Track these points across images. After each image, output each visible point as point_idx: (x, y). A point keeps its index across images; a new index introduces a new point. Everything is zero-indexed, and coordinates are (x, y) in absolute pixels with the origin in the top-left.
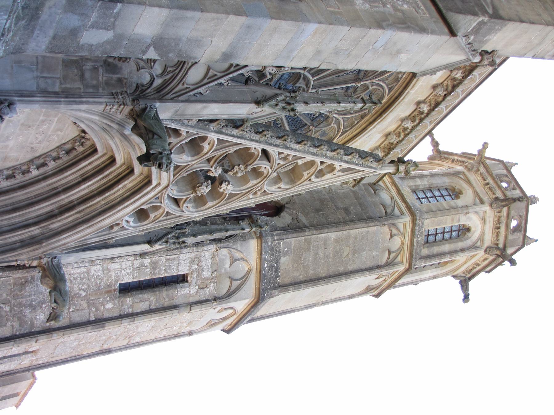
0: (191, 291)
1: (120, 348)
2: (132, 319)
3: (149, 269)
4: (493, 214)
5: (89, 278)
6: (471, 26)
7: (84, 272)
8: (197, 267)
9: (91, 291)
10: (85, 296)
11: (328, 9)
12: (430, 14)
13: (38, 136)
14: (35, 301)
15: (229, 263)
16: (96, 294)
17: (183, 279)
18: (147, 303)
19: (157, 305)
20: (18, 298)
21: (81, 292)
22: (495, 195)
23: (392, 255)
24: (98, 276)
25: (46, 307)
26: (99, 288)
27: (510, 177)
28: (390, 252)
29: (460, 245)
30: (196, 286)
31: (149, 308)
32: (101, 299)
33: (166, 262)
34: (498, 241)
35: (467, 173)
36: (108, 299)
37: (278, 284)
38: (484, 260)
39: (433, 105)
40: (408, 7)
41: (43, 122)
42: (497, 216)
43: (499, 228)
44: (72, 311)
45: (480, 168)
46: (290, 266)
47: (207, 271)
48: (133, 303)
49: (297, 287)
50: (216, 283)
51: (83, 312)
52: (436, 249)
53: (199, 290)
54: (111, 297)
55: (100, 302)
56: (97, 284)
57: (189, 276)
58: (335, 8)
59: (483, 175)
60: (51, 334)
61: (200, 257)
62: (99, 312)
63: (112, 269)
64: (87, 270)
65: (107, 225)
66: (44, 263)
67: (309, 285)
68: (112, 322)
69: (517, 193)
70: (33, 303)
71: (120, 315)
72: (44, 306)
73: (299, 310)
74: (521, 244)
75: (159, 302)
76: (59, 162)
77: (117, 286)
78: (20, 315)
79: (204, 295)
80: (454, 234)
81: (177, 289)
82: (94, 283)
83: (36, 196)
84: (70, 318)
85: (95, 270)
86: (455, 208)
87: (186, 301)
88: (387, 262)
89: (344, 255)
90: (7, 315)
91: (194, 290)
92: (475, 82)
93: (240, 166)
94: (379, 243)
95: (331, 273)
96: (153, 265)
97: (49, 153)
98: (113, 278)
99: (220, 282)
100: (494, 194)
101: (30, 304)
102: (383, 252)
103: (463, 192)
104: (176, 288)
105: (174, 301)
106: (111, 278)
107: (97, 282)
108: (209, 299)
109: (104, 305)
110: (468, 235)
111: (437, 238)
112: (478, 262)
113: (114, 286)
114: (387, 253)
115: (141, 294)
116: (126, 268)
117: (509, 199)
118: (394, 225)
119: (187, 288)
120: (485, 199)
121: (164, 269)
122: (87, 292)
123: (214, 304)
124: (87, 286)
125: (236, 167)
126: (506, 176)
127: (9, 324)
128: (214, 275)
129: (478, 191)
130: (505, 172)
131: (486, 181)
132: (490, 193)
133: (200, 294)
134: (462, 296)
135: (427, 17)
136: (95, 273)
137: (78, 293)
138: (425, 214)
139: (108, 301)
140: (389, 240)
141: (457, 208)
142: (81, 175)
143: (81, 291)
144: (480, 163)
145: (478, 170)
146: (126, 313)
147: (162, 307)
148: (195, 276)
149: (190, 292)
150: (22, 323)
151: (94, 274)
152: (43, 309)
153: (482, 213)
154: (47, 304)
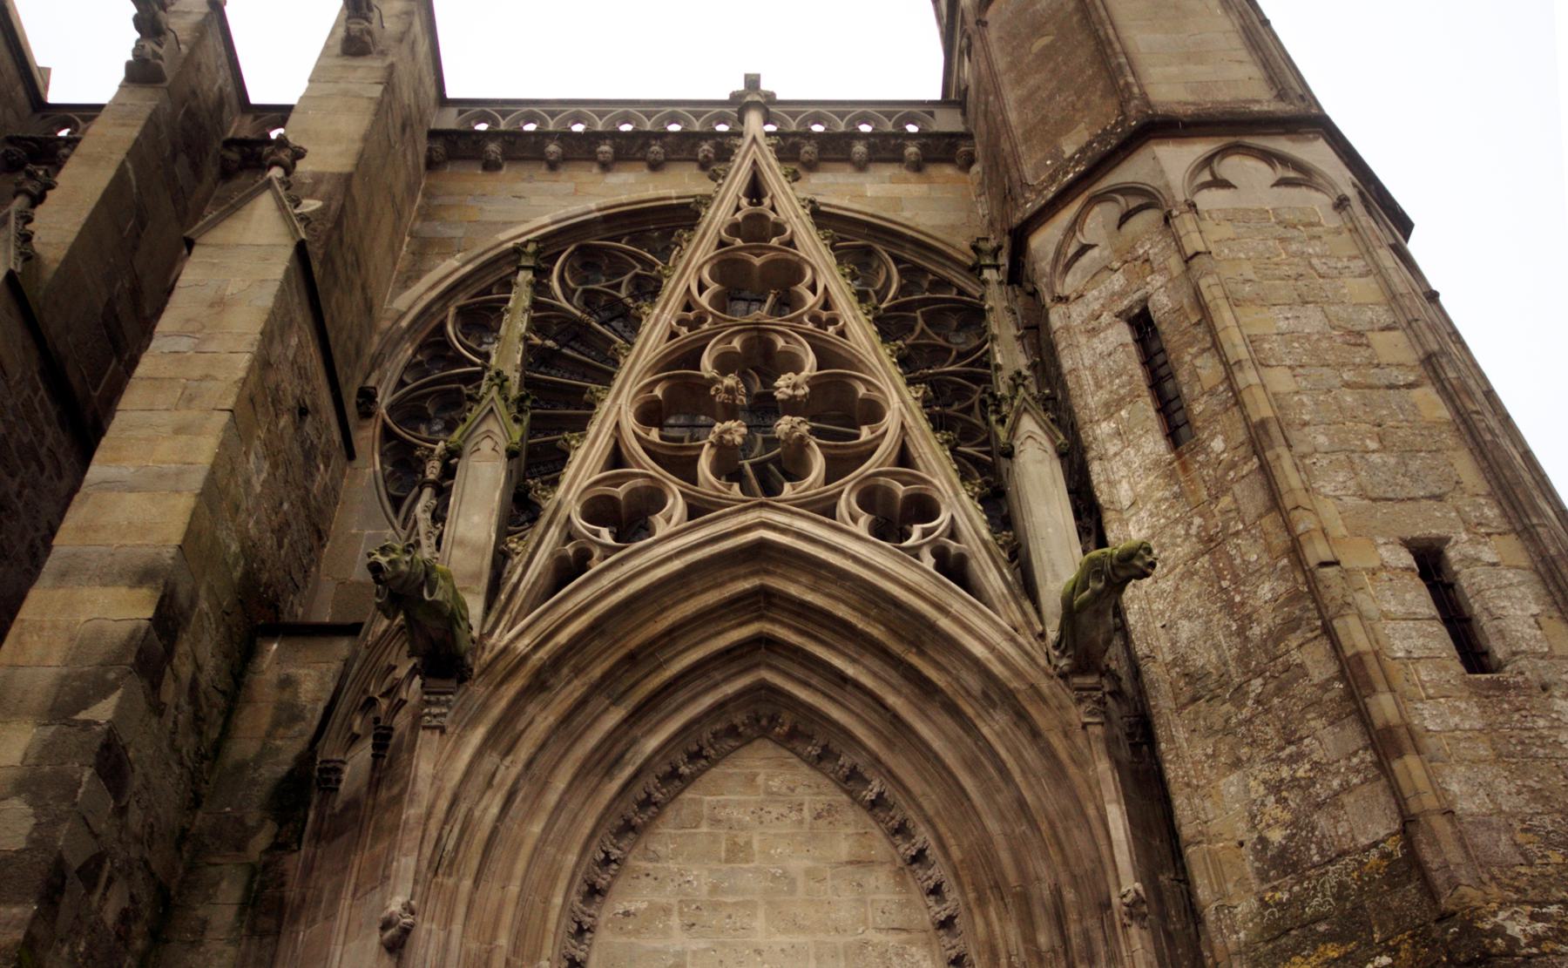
0: (1159, 284)
1: (1414, 340)
10: (1201, 515)
13: (774, 815)
14: (1228, 627)
17: (1142, 323)
20: (1228, 671)
21: (1193, 531)
24: (1151, 515)
25: (1241, 593)
39: (692, 141)
41: (716, 822)
44: (1243, 522)
54: (1197, 454)
56: (1171, 506)
63: (1130, 493)
70: (1234, 628)
72: (1238, 599)
76: (835, 746)
78: (1270, 644)
84: (1260, 516)
90: (1272, 676)
92: (626, 112)
96: (1113, 409)
101: (1239, 635)
109: (1218, 455)
113: (1170, 464)
127: (1296, 657)
139: (1207, 455)
150: (1291, 625)
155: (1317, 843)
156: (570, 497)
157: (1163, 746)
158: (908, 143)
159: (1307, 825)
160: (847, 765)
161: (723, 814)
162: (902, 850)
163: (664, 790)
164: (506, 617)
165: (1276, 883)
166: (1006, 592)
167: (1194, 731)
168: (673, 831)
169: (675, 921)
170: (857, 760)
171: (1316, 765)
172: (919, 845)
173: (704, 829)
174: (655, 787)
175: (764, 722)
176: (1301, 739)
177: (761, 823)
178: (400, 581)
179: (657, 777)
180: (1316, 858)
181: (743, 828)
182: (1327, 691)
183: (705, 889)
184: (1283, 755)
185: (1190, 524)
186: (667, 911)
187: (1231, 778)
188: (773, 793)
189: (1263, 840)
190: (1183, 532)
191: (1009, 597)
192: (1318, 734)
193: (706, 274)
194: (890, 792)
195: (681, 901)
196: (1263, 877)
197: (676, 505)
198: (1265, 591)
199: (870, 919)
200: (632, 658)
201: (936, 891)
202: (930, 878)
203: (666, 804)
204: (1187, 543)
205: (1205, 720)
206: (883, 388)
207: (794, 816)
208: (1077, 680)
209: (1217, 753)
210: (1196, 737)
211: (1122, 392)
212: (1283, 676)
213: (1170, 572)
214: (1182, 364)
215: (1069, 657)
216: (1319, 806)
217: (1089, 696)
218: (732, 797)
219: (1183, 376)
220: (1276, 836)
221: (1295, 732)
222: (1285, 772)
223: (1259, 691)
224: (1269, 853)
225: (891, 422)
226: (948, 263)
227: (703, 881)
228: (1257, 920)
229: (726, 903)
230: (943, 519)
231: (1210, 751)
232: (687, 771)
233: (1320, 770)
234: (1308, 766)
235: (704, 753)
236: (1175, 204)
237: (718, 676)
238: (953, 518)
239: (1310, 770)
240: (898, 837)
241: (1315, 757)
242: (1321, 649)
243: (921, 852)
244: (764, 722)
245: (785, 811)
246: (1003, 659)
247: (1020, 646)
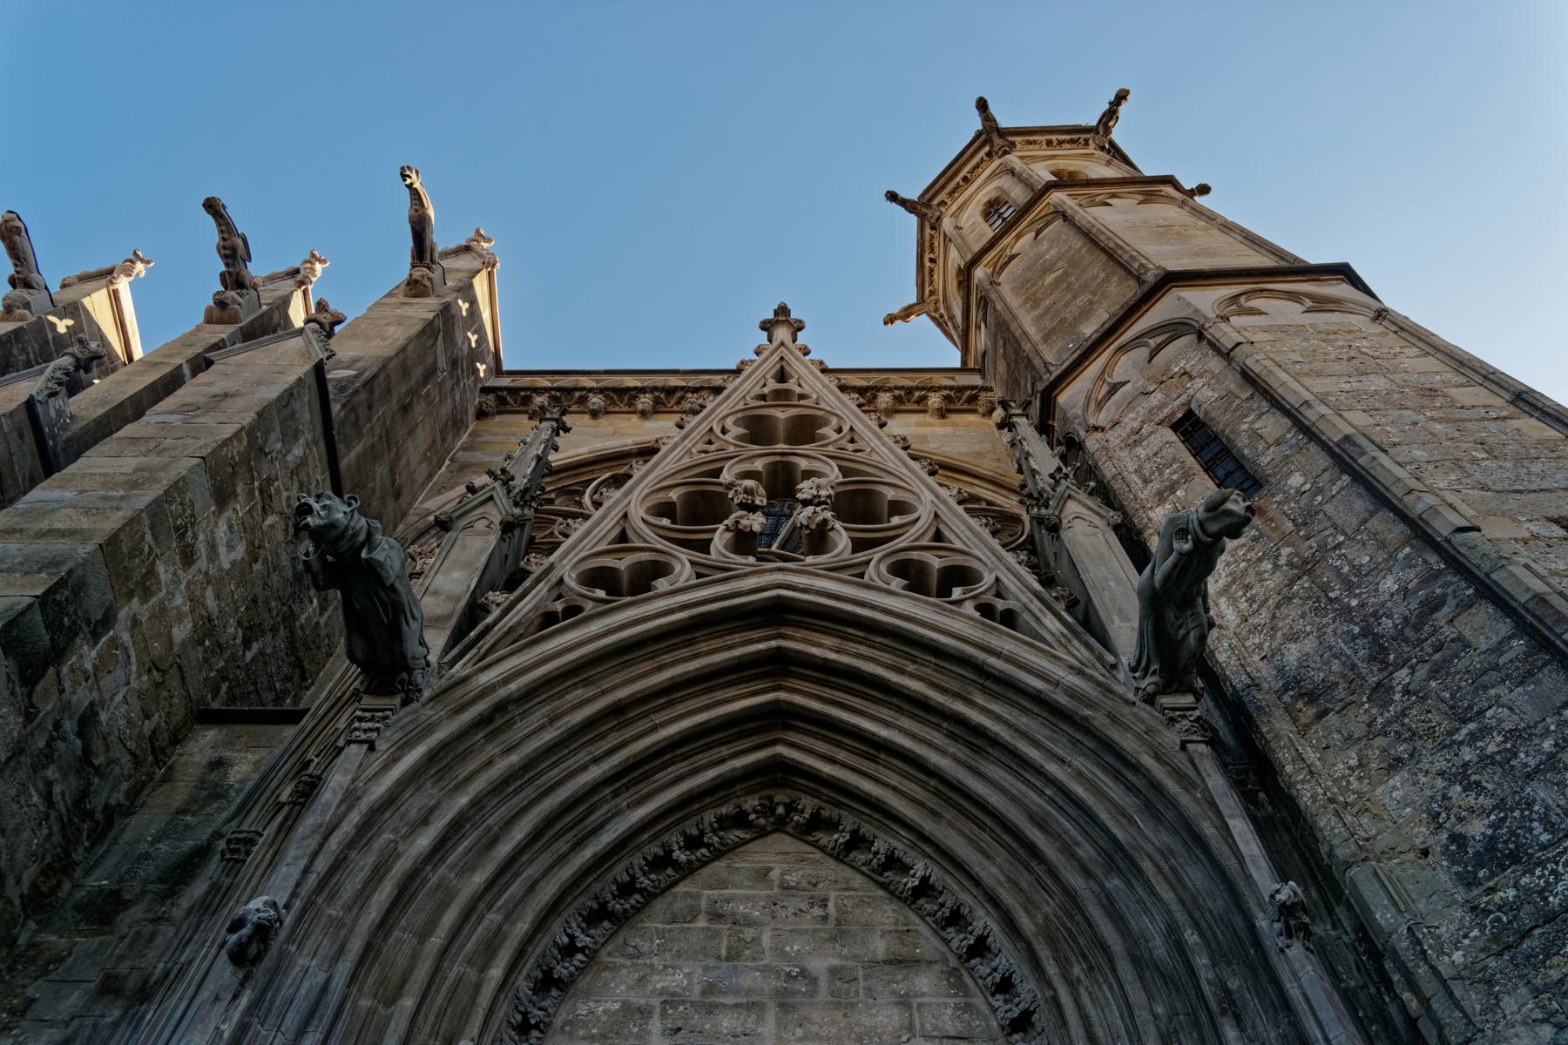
13: (792, 910)
17: (1190, 426)
21: (1283, 561)
25: (1356, 596)
28: (1038, 233)
43: (965, 179)
44: (1345, 534)
55: (1292, 505)
57: (1174, 420)
60: (1421, 519)
65: (927, 603)
66: (1155, 679)
70: (1357, 630)
72: (1354, 603)
76: (867, 829)
83: (982, 826)
97: (864, 869)
100: (932, 237)
101: (1365, 636)
127: (1449, 632)
134: (1123, 110)
142: (874, 760)
152: (1364, 596)
155: (1540, 820)
156: (565, 562)
157: (1289, 769)
158: (932, 394)
159: (1518, 803)
160: (882, 851)
161: (727, 908)
162: (955, 944)
163: (653, 876)
164: (474, 651)
165: (1491, 884)
166: (1065, 631)
167: (1327, 747)
168: (660, 926)
169: (655, 1025)
170: (895, 843)
171: (1511, 734)
172: (978, 932)
173: (701, 923)
174: (641, 869)
175: (780, 810)
176: (1481, 712)
177: (774, 917)
178: (334, 533)
179: (645, 859)
180: (1545, 837)
181: (751, 924)
182: (1503, 653)
183: (697, 989)
184: (1459, 737)
185: (1277, 557)
186: (645, 1012)
187: (1391, 782)
188: (788, 888)
189: (1458, 839)
190: (1270, 566)
191: (1070, 636)
192: (1504, 700)
193: (729, 422)
194: (936, 875)
195: (665, 1002)
196: (1469, 881)
197: (683, 570)
198: (1389, 584)
199: (918, 1027)
200: (618, 711)
201: (1005, 986)
202: (995, 970)
203: (655, 896)
204: (1278, 574)
205: (1339, 732)
206: (916, 490)
207: (817, 911)
208: (1166, 700)
209: (1365, 761)
210: (1330, 755)
211: (1175, 477)
212: (1437, 656)
213: (1260, 606)
214: (1239, 434)
215: (1154, 673)
216: (1529, 777)
217: (1186, 717)
218: (739, 892)
219: (1242, 442)
220: (1477, 829)
221: (1471, 707)
222: (1468, 754)
223: (1407, 680)
224: (1470, 851)
225: (924, 513)
226: (976, 482)
227: (695, 980)
228: (1476, 932)
229: (724, 1005)
230: (988, 579)
231: (1353, 762)
232: (683, 858)
233: (1520, 737)
234: (1499, 739)
235: (706, 840)
236: (1207, 319)
237: (724, 751)
238: (997, 579)
239: (1505, 742)
240: (950, 929)
241: (1508, 726)
242: (1483, 612)
243: (982, 940)
244: (780, 810)
245: (804, 906)
246: (1071, 692)
247: (1090, 678)
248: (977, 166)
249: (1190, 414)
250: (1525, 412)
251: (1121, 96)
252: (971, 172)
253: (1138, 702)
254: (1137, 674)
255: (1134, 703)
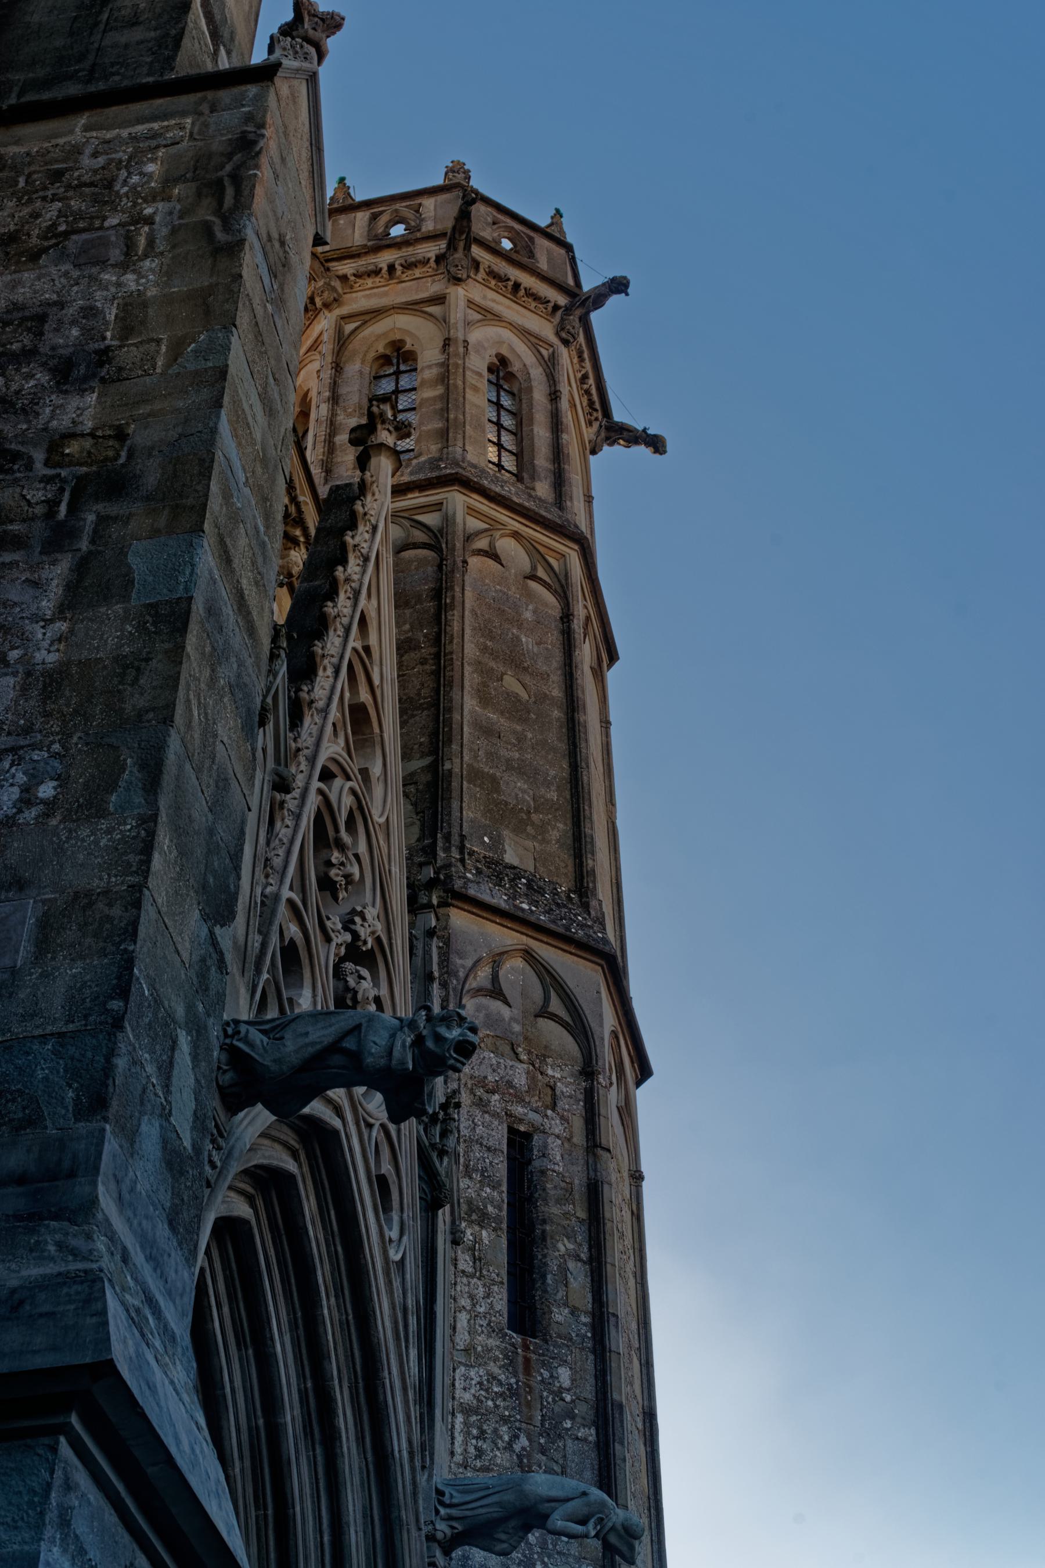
0: (557, 1131)
2: (612, 1319)
3: (484, 1233)
4: (477, 284)
5: (483, 1414)
6: (203, 33)
7: (466, 1424)
8: (497, 1097)
9: (518, 1417)
11: (159, 370)
12: (184, 114)
15: (499, 1003)
16: (529, 1405)
18: (571, 1265)
19: (579, 1238)
21: (517, 1447)
22: (429, 259)
23: (541, 573)
24: (480, 1383)
26: (512, 1392)
27: (381, 209)
28: (533, 577)
29: (539, 395)
30: (546, 1116)
31: (585, 1263)
32: (545, 1394)
33: (471, 1178)
34: (549, 301)
35: (344, 310)
36: (546, 1374)
37: (575, 892)
38: (579, 357)
40: (153, 160)
42: (486, 277)
43: (517, 286)
45: (340, 273)
46: (529, 844)
47: (511, 1072)
48: (566, 1305)
49: (589, 846)
50: (545, 1056)
51: (570, 1457)
52: (542, 460)
53: (559, 1109)
54: (544, 1364)
55: (550, 1399)
56: (501, 1395)
58: (158, 352)
59: (362, 269)
61: (472, 1077)
62: (576, 1411)
64: (462, 1412)
66: (448, 1531)
67: (587, 813)
68: (612, 1379)
69: (432, 208)
71: (594, 1351)
73: (618, 869)
74: (563, 252)
75: (573, 1231)
77: (517, 1339)
79: (572, 1101)
80: (506, 401)
81: (548, 1170)
82: (498, 1403)
85: (465, 1389)
86: (448, 371)
87: (580, 1154)
88: (554, 593)
89: (524, 695)
91: (557, 1127)
93: (334, 861)
94: (504, 593)
95: (563, 746)
96: (474, 1217)
98: (492, 1342)
99: (546, 1047)
100: (425, 262)
102: (530, 595)
103: (398, 337)
104: (543, 1172)
105: (576, 1188)
106: (492, 1349)
107: (496, 1393)
108: (585, 1089)
109: (561, 1390)
110: (516, 367)
111: (509, 448)
112: (579, 375)
114: (533, 585)
115: (544, 1277)
116: (472, 1297)
117: (454, 228)
118: (469, 538)
119: (550, 1140)
120: (433, 288)
121: (488, 1190)
122: (519, 1429)
123: (601, 1080)
124: (504, 1425)
125: (333, 872)
126: (374, 217)
128: (524, 1057)
129: (404, 300)
130: (362, 217)
131: (381, 269)
132: (417, 272)
133: (569, 1111)
134: (642, 451)
135: (193, 124)
136: (473, 1391)
137: (520, 1457)
138: (450, 449)
139: (552, 1376)
140: (502, 565)
141: (448, 366)
143: (515, 1446)
144: (326, 265)
145: (344, 278)
146: (589, 1335)
147: (587, 1226)
148: (519, 1110)
149: (558, 1137)
151: (474, 1396)
153: (470, 311)
154: (536, 1556)
215: (452, 1528)
248: (536, 298)
249: (528, 1136)
250: (645, 1435)
251: (657, 444)
252: (530, 294)
253: (423, 1533)
254: (443, 1511)
255: (420, 1529)
